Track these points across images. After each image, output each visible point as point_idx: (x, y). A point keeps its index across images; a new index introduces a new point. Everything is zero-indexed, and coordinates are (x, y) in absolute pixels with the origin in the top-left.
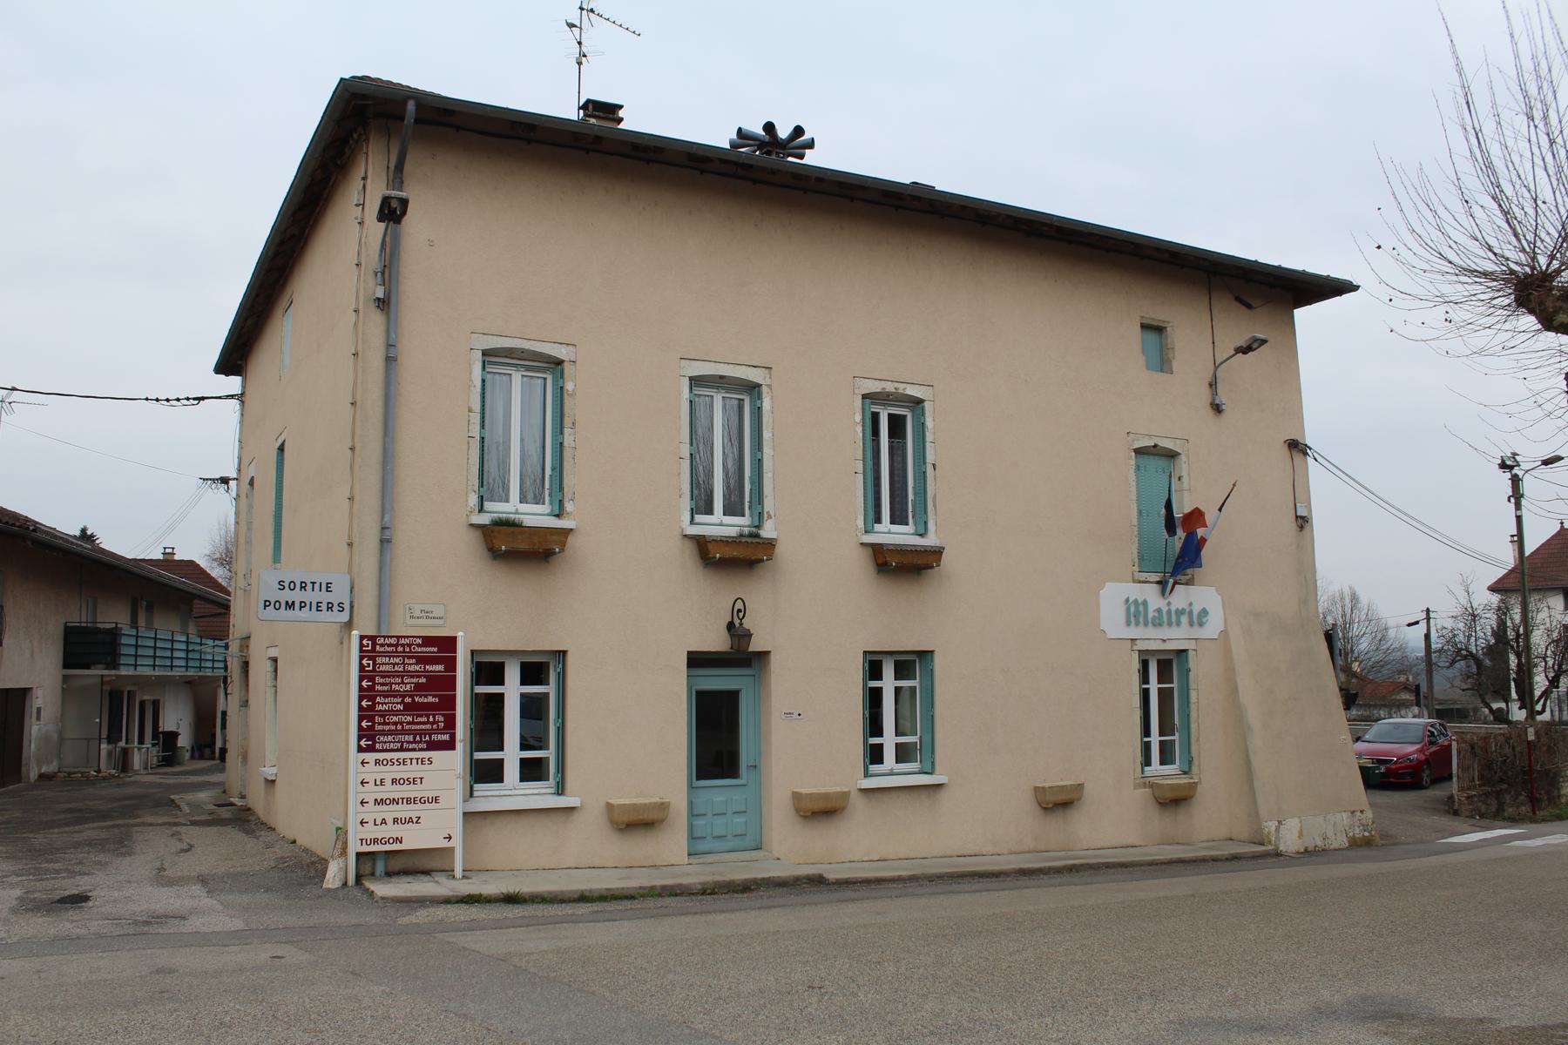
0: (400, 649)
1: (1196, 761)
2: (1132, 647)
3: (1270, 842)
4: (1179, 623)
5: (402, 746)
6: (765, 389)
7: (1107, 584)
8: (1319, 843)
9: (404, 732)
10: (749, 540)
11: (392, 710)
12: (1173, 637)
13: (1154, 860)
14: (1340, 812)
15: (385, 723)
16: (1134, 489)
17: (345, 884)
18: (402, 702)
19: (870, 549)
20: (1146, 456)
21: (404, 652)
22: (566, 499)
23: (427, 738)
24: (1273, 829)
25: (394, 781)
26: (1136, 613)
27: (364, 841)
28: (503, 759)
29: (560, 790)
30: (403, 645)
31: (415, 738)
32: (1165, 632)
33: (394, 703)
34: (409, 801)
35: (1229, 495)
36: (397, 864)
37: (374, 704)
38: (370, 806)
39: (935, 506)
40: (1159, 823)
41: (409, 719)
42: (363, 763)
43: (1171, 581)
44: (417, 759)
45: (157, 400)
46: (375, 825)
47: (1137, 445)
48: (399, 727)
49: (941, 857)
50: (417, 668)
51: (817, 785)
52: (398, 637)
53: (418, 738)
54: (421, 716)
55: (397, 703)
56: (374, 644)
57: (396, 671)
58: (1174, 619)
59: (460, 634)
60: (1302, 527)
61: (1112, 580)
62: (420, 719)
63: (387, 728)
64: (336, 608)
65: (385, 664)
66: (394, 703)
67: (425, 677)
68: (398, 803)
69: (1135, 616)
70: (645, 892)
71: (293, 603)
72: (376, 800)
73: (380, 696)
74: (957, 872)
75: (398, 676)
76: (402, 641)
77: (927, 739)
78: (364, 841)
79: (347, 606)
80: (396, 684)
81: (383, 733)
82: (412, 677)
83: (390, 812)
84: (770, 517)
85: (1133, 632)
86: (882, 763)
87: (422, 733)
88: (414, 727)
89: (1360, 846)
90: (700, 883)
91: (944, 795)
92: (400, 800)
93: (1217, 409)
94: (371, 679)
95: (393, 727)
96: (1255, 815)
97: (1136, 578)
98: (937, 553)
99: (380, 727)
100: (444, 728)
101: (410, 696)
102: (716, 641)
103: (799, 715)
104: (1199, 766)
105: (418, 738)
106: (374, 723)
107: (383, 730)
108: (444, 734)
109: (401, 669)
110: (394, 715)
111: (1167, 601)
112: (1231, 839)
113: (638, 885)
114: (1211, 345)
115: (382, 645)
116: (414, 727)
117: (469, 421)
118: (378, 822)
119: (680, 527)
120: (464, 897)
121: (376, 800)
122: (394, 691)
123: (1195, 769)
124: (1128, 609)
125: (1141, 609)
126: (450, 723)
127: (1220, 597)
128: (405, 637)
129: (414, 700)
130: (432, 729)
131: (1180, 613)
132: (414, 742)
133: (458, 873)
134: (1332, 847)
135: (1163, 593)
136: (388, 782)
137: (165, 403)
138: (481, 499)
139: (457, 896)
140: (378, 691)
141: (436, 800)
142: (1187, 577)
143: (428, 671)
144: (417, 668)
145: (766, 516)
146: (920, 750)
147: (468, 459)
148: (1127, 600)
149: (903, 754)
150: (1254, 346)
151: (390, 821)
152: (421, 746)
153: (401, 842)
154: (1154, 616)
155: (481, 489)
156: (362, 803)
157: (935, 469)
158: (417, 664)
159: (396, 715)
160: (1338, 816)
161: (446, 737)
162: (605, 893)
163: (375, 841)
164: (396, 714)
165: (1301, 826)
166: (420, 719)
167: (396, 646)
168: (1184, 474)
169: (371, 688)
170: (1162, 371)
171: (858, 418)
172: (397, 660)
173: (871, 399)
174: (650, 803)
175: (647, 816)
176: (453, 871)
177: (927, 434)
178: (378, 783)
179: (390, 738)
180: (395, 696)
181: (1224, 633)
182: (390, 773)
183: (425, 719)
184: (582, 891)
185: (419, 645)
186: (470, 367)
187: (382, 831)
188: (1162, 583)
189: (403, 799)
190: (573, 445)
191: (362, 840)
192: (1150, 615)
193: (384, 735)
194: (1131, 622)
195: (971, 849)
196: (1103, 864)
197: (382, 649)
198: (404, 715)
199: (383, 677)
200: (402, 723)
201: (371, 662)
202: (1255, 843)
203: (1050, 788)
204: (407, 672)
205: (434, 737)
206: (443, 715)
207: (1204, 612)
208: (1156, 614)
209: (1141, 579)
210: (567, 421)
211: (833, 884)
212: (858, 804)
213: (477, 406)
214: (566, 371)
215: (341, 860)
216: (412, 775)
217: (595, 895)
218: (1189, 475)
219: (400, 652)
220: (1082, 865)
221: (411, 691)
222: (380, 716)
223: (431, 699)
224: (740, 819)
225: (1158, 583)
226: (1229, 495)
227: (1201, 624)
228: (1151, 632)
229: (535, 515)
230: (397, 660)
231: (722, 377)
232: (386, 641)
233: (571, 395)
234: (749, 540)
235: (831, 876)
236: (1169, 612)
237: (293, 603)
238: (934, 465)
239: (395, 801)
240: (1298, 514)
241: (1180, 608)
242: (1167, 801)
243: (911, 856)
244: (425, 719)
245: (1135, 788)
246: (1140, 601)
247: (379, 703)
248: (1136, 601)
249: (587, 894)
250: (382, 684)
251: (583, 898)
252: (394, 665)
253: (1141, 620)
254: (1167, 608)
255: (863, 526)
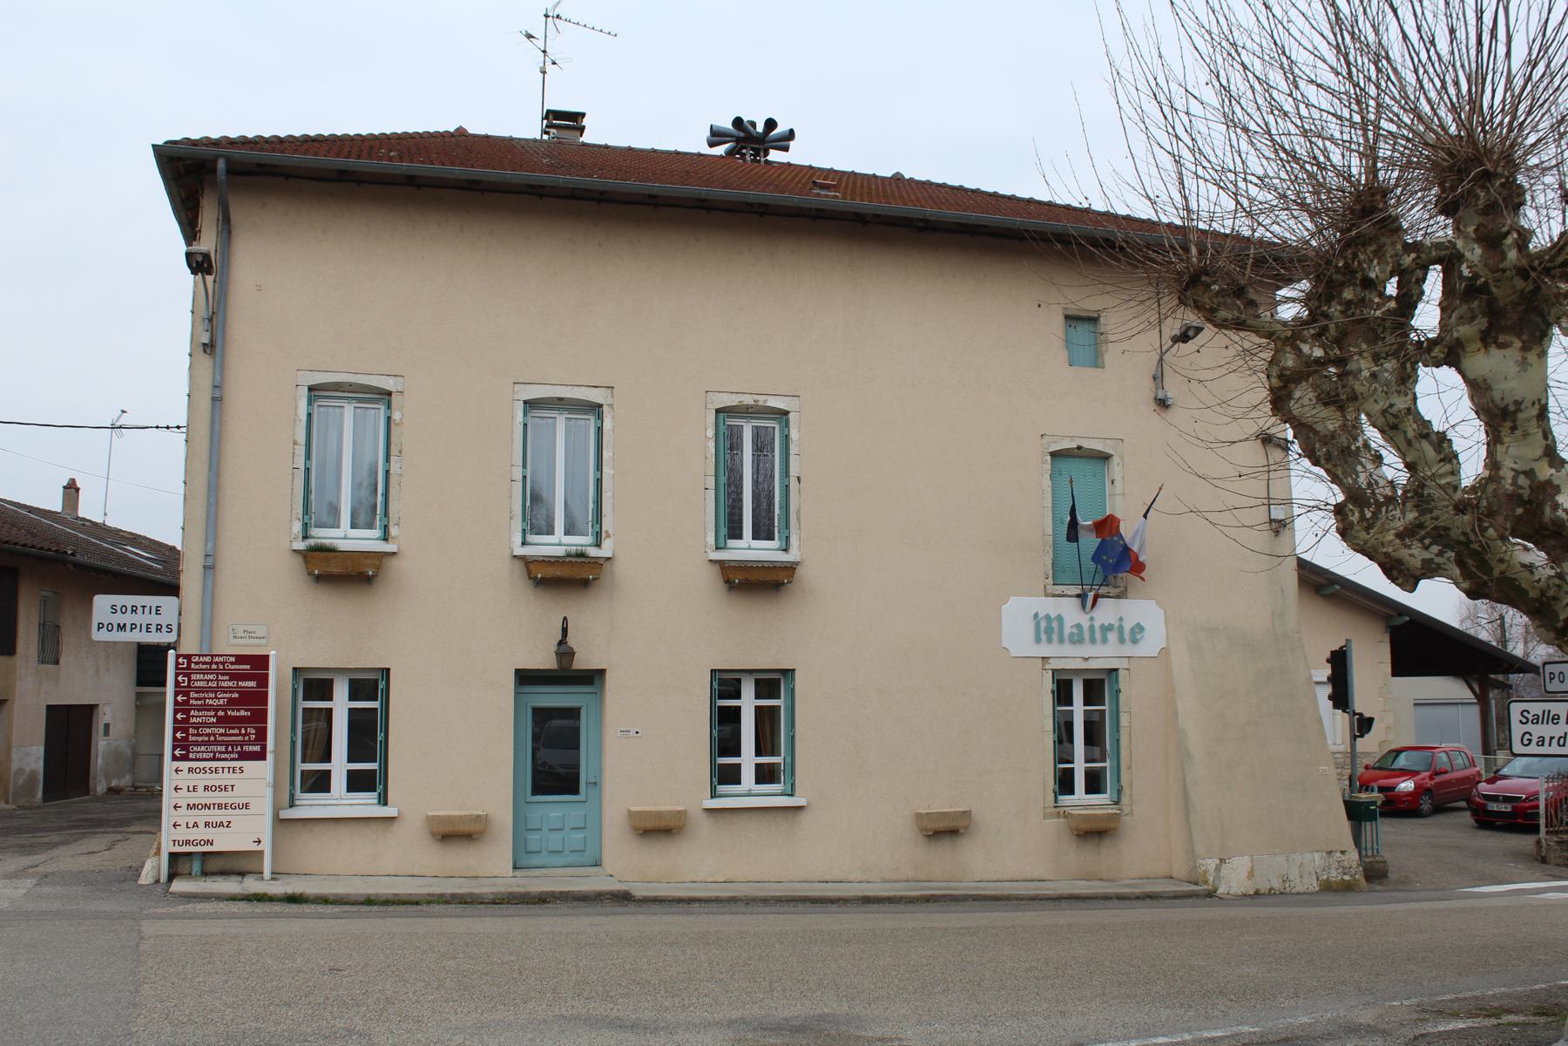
0: (214, 666)
1: (1126, 791)
2: (1043, 665)
3: (1206, 882)
4: (1105, 640)
5: (214, 755)
6: (605, 408)
7: (1012, 599)
8: (1277, 885)
9: (216, 743)
10: (574, 560)
11: (206, 723)
12: (1100, 656)
13: (1038, 895)
14: (1311, 852)
15: (198, 735)
16: (1049, 496)
17: (157, 881)
18: (216, 715)
19: (718, 566)
20: (1070, 459)
21: (218, 669)
22: (391, 524)
23: (239, 749)
24: (1212, 867)
25: (206, 788)
26: (1047, 629)
27: (177, 843)
28: (330, 771)
29: (383, 800)
30: (217, 663)
31: (227, 749)
32: (1087, 650)
33: (207, 716)
34: (220, 806)
35: (1154, 500)
36: (213, 865)
37: (189, 717)
38: (183, 810)
39: (798, 519)
40: (1078, 857)
41: (222, 731)
42: (176, 771)
43: (1091, 595)
44: (229, 768)
45: (168, 428)
46: (187, 827)
47: (1054, 448)
48: (212, 738)
49: (799, 882)
50: (230, 684)
51: (662, 802)
52: (212, 656)
53: (230, 749)
54: (233, 728)
55: (210, 716)
56: (189, 662)
57: (210, 687)
58: (1098, 635)
59: (272, 653)
60: (1277, 533)
61: (1017, 594)
62: (232, 731)
63: (200, 739)
64: (164, 629)
65: (199, 680)
66: (207, 716)
67: (237, 692)
68: (209, 809)
69: (1046, 632)
70: (432, 898)
71: (125, 625)
72: (188, 805)
73: (194, 709)
74: (786, 896)
75: (212, 692)
76: (216, 659)
77: (789, 760)
78: (177, 843)
79: (175, 628)
80: (209, 698)
81: (197, 744)
82: (225, 692)
83: (201, 816)
84: (608, 536)
85: (1045, 650)
86: (740, 784)
87: (233, 744)
88: (226, 739)
89: (1335, 891)
90: (492, 893)
91: (804, 818)
92: (212, 806)
93: (1163, 404)
94: (186, 694)
95: (206, 739)
96: (1191, 853)
97: (1050, 592)
98: (790, 569)
99: (194, 738)
100: (255, 740)
101: (223, 710)
102: (544, 659)
103: (637, 733)
104: (1131, 796)
105: (230, 749)
106: (188, 734)
107: (197, 741)
108: (255, 745)
109: (215, 685)
110: (207, 727)
111: (1089, 616)
112: (1171, 878)
113: (426, 892)
114: (1158, 334)
115: (197, 663)
116: (226, 739)
117: (294, 453)
118: (190, 825)
119: (510, 548)
120: (249, 895)
121: (188, 805)
122: (208, 705)
123: (1125, 800)
124: (1037, 625)
125: (1055, 625)
126: (262, 735)
127: (1162, 611)
128: (219, 656)
129: (226, 713)
130: (244, 741)
131: (1106, 629)
132: (227, 752)
133: (267, 874)
134: (1294, 891)
135: (1083, 606)
136: (200, 789)
137: (176, 430)
138: (306, 526)
139: (243, 894)
140: (192, 705)
141: (246, 806)
142: (1118, 590)
143: (241, 687)
144: (230, 684)
145: (604, 535)
146: (784, 771)
147: (293, 489)
148: (1036, 615)
149: (765, 775)
150: (1191, 333)
151: (201, 825)
152: (233, 756)
153: (212, 844)
154: (1071, 632)
155: (306, 517)
156: (175, 807)
157: (799, 482)
158: (230, 680)
159: (209, 728)
160: (1308, 856)
161: (257, 748)
162: (391, 898)
163: (187, 842)
164: (209, 725)
165: (1253, 867)
166: (232, 731)
167: (211, 663)
168: (1117, 477)
169: (186, 703)
170: (1097, 367)
171: (711, 433)
172: (211, 677)
173: (725, 412)
174: (466, 816)
175: (462, 828)
176: (262, 873)
177: (792, 446)
178: (191, 789)
179: (203, 748)
180: (209, 710)
181: (1164, 651)
182: (202, 780)
183: (237, 731)
184: (368, 895)
185: (232, 663)
186: (296, 402)
187: (193, 835)
188: (1082, 597)
189: (214, 804)
190: (399, 471)
191: (174, 841)
192: (1067, 631)
193: (198, 745)
194: (1040, 639)
195: (836, 875)
196: (970, 895)
197: (197, 667)
198: (217, 727)
199: (197, 692)
200: (214, 735)
201: (186, 679)
202: (1191, 883)
203: (927, 814)
204: (221, 687)
205: (246, 748)
206: (254, 728)
207: (1139, 628)
208: (1075, 631)
209: (1057, 593)
210: (394, 450)
211: (640, 901)
212: (705, 826)
213: (302, 438)
214: (393, 402)
215: (155, 859)
216: (223, 783)
217: (382, 899)
218: (1123, 478)
219: (214, 669)
220: (942, 896)
221: (224, 705)
222: (195, 728)
223: (243, 713)
224: (580, 835)
225: (1078, 596)
226: (1154, 500)
227: (1135, 641)
228: (1068, 650)
229: (364, 540)
230: (211, 677)
231: (560, 399)
232: (201, 659)
233: (397, 424)
234: (574, 560)
235: (639, 891)
236: (1092, 628)
237: (125, 625)
238: (799, 478)
239: (207, 807)
240: (1272, 518)
241: (1106, 624)
242: (1082, 833)
243: (809, 879)
244: (237, 731)
245: (1044, 818)
246: (1053, 617)
247: (193, 716)
248: (1047, 617)
249: (374, 898)
250: (196, 699)
251: (369, 901)
252: (208, 681)
253: (1055, 637)
254: (1089, 624)
255: (713, 543)
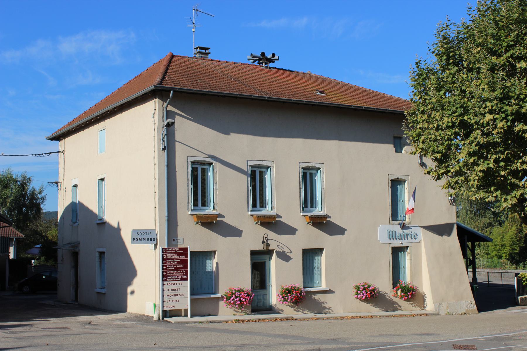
0: (173, 252)
9: (174, 276)
15: (169, 273)
17: (159, 319)
25: (172, 290)
30: (174, 251)
34: (176, 295)
41: (176, 272)
45: (36, 155)
48: (173, 274)
50: (178, 257)
53: (178, 277)
54: (179, 271)
56: (166, 250)
59: (188, 247)
62: (178, 272)
63: (170, 274)
64: (153, 240)
71: (141, 239)
76: (173, 249)
79: (156, 239)
81: (169, 276)
82: (176, 260)
87: (179, 276)
88: (177, 274)
95: (171, 274)
100: (185, 274)
101: (176, 265)
102: (260, 247)
105: (178, 277)
115: (168, 251)
116: (177, 274)
118: (168, 302)
132: (177, 278)
136: (170, 290)
137: (38, 156)
141: (183, 295)
144: (178, 257)
151: (171, 301)
158: (177, 256)
161: (185, 277)
166: (178, 272)
167: (172, 251)
179: (171, 277)
180: (172, 265)
183: (180, 272)
185: (178, 250)
197: (168, 252)
199: (169, 260)
200: (174, 273)
205: (182, 277)
216: (177, 288)
222: (168, 271)
223: (181, 266)
230: (172, 255)
237: (141, 239)
239: (172, 295)
244: (180, 272)
250: (168, 262)
252: (171, 256)
